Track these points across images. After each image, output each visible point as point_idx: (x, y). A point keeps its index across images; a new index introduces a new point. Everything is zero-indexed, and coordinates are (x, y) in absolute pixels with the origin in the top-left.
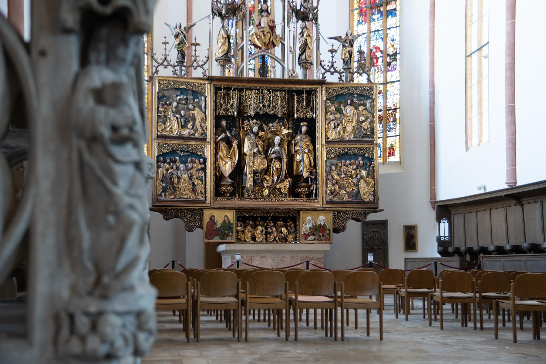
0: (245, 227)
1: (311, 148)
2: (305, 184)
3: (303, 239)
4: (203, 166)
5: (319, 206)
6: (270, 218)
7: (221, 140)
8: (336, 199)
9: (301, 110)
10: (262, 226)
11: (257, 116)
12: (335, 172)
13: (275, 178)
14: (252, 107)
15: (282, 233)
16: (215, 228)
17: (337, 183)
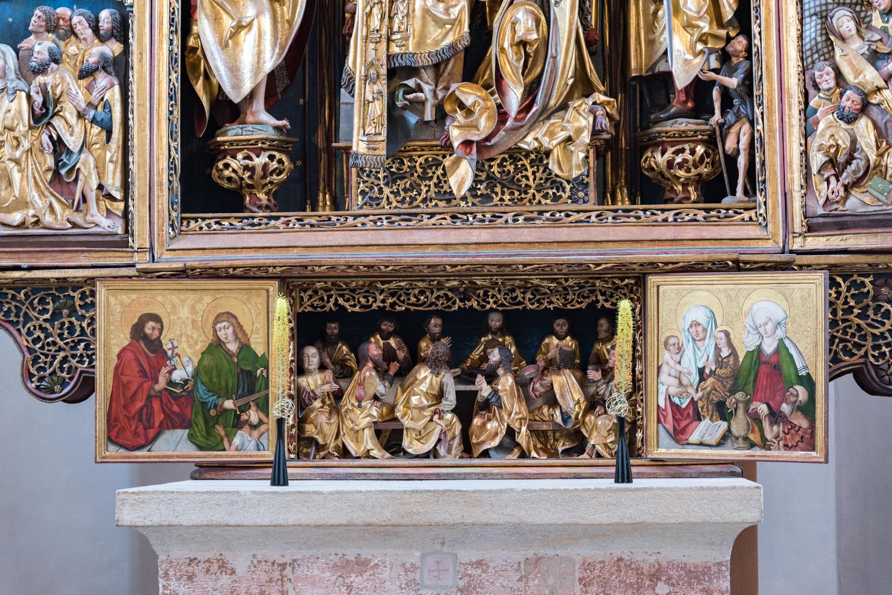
0: (344, 373)
2: (684, 125)
3: (665, 438)
4: (113, 48)
5: (766, 241)
6: (495, 321)
8: (856, 203)
10: (435, 365)
13: (514, 96)
15: (553, 402)
16: (162, 384)
17: (865, 107)
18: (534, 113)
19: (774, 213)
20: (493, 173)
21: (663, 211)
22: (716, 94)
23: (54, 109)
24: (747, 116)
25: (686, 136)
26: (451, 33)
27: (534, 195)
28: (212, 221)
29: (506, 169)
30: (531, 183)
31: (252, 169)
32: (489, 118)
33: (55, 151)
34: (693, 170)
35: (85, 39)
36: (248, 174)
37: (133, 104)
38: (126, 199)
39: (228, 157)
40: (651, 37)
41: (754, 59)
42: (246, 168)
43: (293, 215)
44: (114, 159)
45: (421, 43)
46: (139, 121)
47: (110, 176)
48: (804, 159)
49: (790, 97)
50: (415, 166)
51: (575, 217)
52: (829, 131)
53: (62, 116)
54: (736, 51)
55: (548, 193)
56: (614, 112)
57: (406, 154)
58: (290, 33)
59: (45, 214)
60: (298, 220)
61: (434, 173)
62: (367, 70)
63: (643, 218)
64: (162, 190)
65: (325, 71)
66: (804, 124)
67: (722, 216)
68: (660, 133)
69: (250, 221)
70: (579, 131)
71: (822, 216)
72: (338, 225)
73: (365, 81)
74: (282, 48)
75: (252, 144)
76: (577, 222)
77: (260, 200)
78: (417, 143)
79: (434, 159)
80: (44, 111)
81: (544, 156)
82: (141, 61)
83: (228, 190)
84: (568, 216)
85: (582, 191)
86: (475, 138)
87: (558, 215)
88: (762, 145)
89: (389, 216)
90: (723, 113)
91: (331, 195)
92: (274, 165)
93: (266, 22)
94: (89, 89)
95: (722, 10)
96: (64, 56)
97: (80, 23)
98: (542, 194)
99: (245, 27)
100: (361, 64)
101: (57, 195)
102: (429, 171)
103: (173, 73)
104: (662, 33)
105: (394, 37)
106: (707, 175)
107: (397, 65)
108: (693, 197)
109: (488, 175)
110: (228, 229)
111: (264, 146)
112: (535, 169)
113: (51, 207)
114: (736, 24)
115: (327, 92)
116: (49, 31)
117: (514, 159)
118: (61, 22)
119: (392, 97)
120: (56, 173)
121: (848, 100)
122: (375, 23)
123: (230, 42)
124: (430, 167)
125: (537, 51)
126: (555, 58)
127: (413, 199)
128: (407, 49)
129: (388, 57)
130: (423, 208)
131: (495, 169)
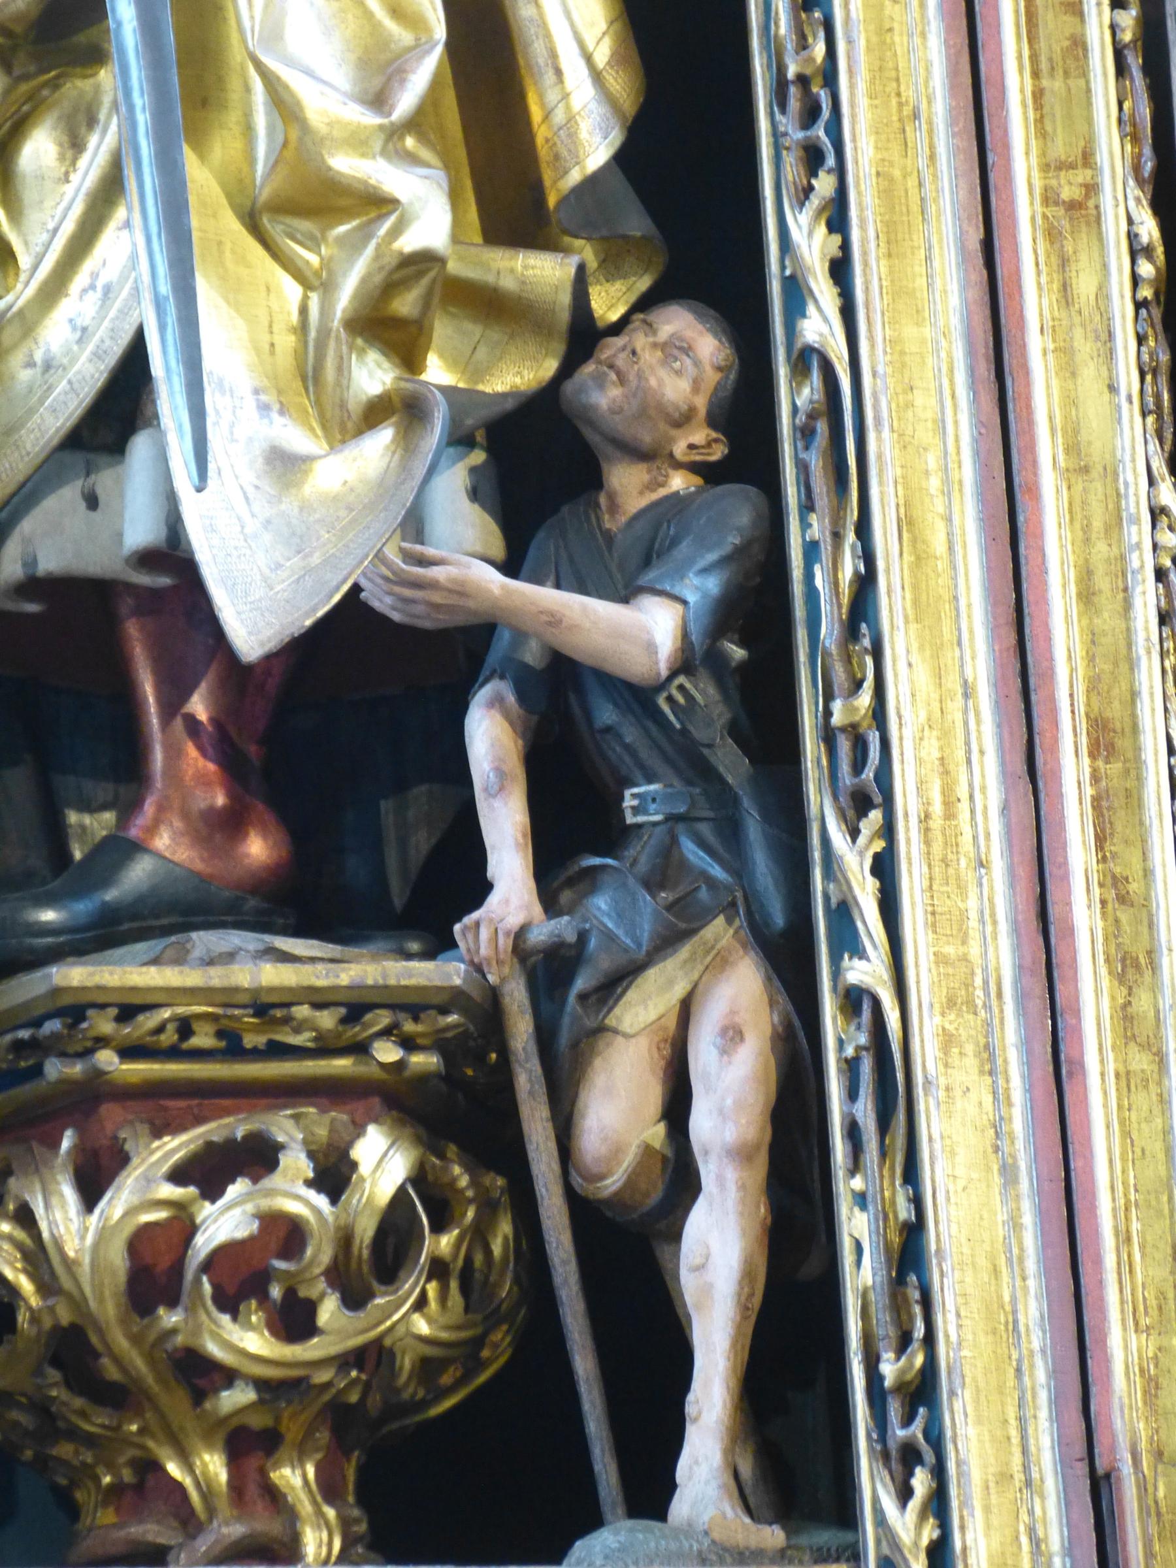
22: (489, 736)
34: (329, 1310)
54: (649, 408)
68: (76, 1010)
106: (428, 1368)
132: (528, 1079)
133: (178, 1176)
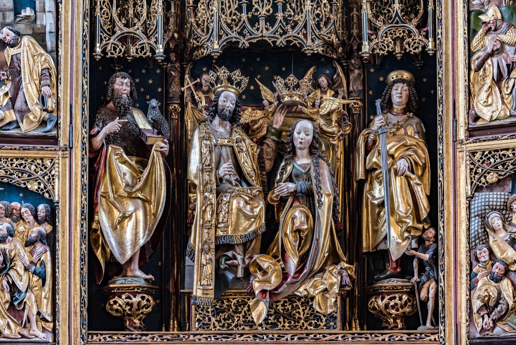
1: (422, 154)
7: (110, 139)
9: (383, 28)
11: (231, 56)
12: (502, 234)
13: (293, 262)
14: (214, 26)
18: (305, 274)
19: (449, 337)
20: (279, 310)
21: (382, 334)
22: (415, 263)
23: (10, 265)
24: (434, 277)
25: (397, 289)
26: (254, 224)
27: (303, 324)
28: (107, 336)
29: (286, 308)
30: (302, 316)
31: (131, 305)
32: (276, 277)
33: (11, 290)
34: (400, 310)
35: (29, 222)
36: (128, 308)
37: (58, 263)
38: (54, 321)
39: (116, 297)
40: (376, 228)
41: (440, 242)
42: (127, 304)
43: (156, 334)
44: (47, 296)
45: (235, 230)
46: (62, 274)
47: (45, 307)
48: (469, 304)
49: (461, 266)
50: (231, 305)
51: (329, 337)
52: (485, 287)
53: (15, 270)
54: (428, 237)
55: (312, 323)
56: (353, 274)
57: (225, 297)
58: (155, 222)
59: (4, 329)
60: (160, 336)
61: (242, 309)
62: (203, 246)
63: (370, 339)
64: (76, 316)
65: (175, 245)
66: (469, 283)
67: (418, 338)
68: (381, 287)
69: (130, 336)
70: (332, 285)
71: (479, 338)
72: (184, 340)
73: (202, 252)
74: (150, 231)
75: (131, 290)
76: (330, 340)
77: (135, 324)
78: (232, 291)
79: (242, 301)
80: (4, 266)
81: (310, 300)
82: (63, 236)
83: (116, 317)
84: (324, 336)
85: (333, 321)
86: (269, 289)
87: (318, 336)
88: (443, 295)
89: (215, 335)
90: (420, 276)
91: (177, 321)
92: (144, 302)
93: (140, 214)
94: (31, 253)
95: (420, 212)
96: (16, 232)
97: (26, 211)
98: (308, 323)
99: (126, 217)
100: (199, 242)
101: (12, 317)
102: (239, 308)
103: (83, 244)
104: (383, 226)
105: (219, 226)
107: (221, 243)
108: (400, 326)
109: (275, 311)
110: (117, 341)
111: (138, 291)
112: (304, 308)
113: (8, 325)
114: (429, 221)
115: (176, 258)
116: (7, 217)
117: (292, 302)
118: (15, 211)
119: (218, 262)
120: (12, 304)
121: (497, 268)
122: (208, 216)
123: (118, 226)
124: (240, 306)
125: (307, 236)
126: (318, 240)
127: (229, 325)
128: (228, 233)
129: (216, 238)
130: (235, 331)
131: (280, 307)
132: (416, 291)
133: (389, 299)
